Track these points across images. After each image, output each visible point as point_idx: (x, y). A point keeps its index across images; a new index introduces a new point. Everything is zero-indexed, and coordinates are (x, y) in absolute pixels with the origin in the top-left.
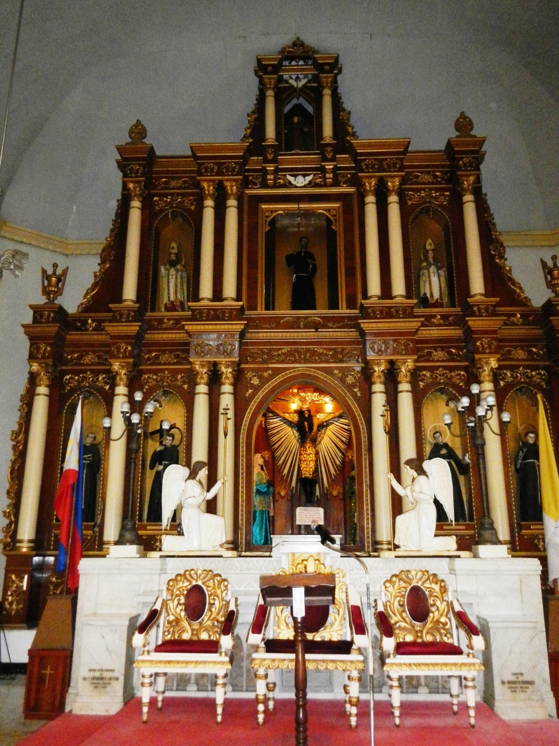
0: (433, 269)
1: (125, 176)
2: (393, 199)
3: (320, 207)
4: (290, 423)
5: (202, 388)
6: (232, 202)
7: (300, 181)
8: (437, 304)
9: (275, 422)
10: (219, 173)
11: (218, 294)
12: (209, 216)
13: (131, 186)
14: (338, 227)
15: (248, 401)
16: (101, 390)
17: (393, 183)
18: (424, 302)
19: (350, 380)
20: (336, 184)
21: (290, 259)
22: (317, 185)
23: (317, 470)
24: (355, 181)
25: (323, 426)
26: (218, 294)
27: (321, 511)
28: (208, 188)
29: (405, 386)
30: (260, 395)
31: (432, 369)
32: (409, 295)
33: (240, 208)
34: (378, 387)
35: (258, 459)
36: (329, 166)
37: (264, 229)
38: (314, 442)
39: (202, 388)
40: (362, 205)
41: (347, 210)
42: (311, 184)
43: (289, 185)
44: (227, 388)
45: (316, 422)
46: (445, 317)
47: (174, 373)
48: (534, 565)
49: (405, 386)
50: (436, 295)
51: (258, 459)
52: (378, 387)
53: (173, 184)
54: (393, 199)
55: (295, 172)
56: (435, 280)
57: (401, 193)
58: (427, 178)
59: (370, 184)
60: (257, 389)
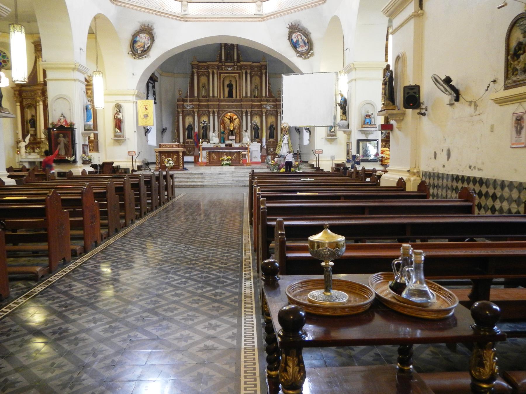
0: (256, 90)
1: (192, 68)
2: (249, 75)
3: (233, 75)
4: (228, 119)
5: (211, 115)
6: (216, 75)
7: (230, 69)
8: (257, 97)
9: (225, 118)
10: (213, 69)
11: (213, 96)
12: (211, 78)
13: (194, 70)
14: (238, 80)
15: (220, 117)
16: (191, 114)
17: (249, 72)
18: (255, 97)
19: (239, 112)
20: (237, 70)
21: (228, 86)
22: (233, 70)
23: (234, 128)
24: (241, 70)
25: (235, 119)
26: (213, 96)
27: (235, 137)
28: (211, 72)
29: (249, 115)
30: (222, 115)
31: (255, 111)
32: (251, 97)
33: (217, 76)
34: (244, 115)
35: (222, 126)
36: (236, 67)
37: (222, 80)
38: (233, 123)
39: (211, 115)
40: (242, 76)
41: (239, 76)
42: (232, 70)
43: (228, 70)
44: (216, 115)
45: (233, 118)
46: (258, 100)
47: (205, 111)
48: (260, 144)
49: (249, 115)
50: (257, 95)
51: (222, 126)
52: (244, 115)
53: (203, 69)
54: (249, 75)
55: (229, 66)
56: (256, 92)
57: (250, 73)
58: (256, 69)
59: (244, 71)
60: (221, 114)
